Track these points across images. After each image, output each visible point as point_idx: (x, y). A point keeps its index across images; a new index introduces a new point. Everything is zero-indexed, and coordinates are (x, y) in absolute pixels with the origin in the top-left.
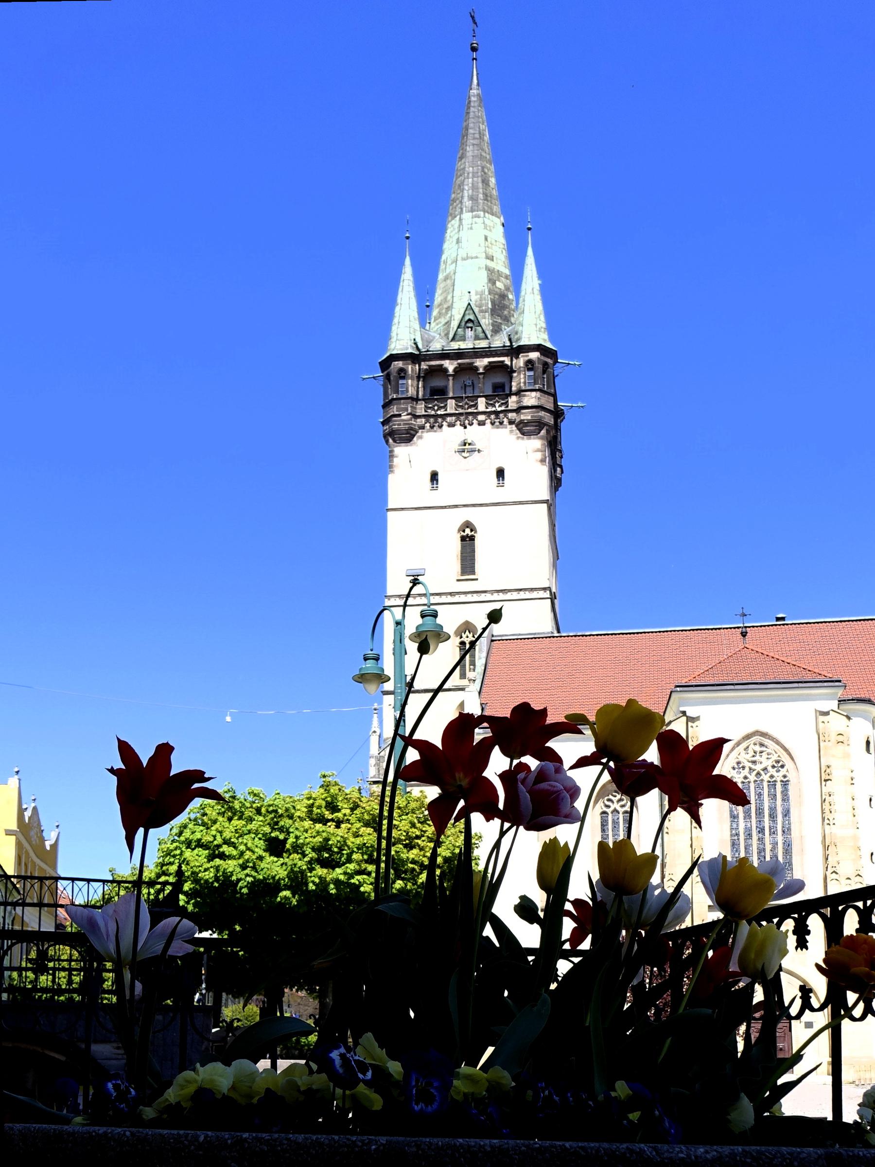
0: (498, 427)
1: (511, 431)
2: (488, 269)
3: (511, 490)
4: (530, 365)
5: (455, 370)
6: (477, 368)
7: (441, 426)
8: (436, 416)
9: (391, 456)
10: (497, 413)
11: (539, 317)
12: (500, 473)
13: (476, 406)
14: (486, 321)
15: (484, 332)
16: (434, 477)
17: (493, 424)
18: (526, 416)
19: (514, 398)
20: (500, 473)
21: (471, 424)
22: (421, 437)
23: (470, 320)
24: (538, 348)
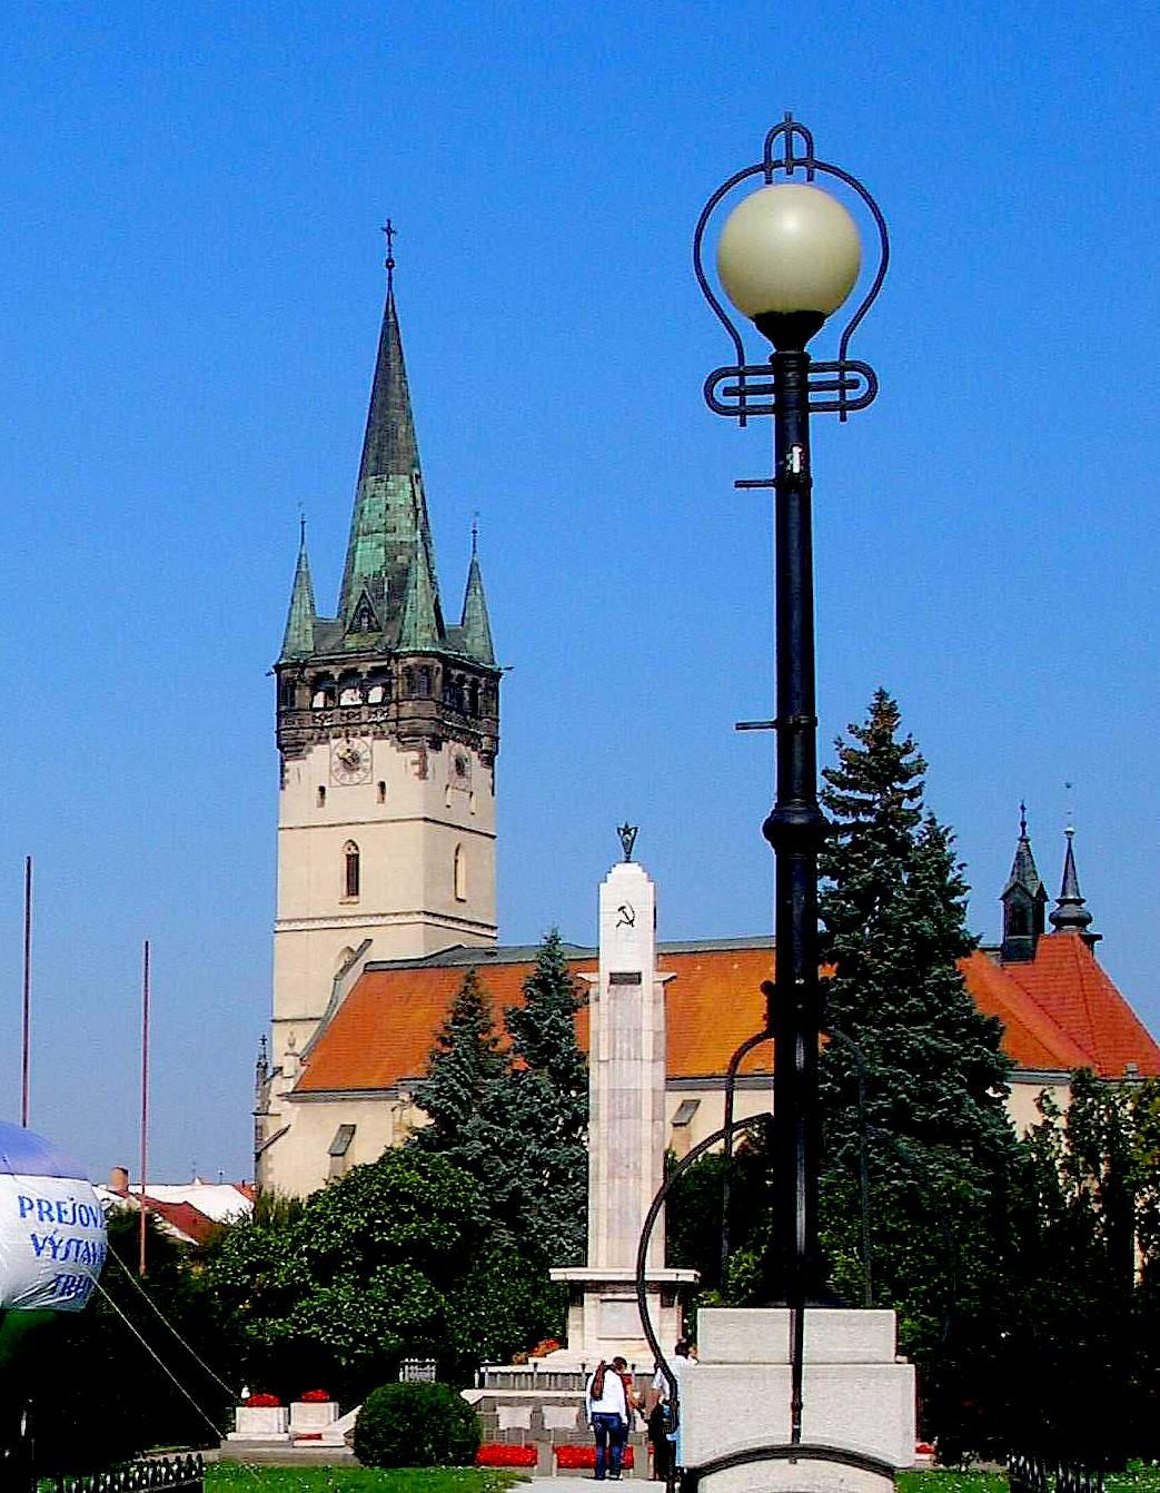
0: (380, 739)
1: (392, 745)
2: (386, 545)
3: (392, 808)
4: (409, 671)
5: (341, 675)
6: (360, 674)
7: (327, 737)
8: (322, 728)
9: (283, 770)
10: (378, 723)
11: (422, 614)
12: (382, 785)
13: (359, 713)
14: (381, 610)
15: (377, 623)
16: (322, 789)
17: (375, 733)
18: (404, 727)
19: (393, 707)
20: (382, 785)
21: (355, 735)
22: (310, 751)
23: (365, 609)
24: (415, 654)
